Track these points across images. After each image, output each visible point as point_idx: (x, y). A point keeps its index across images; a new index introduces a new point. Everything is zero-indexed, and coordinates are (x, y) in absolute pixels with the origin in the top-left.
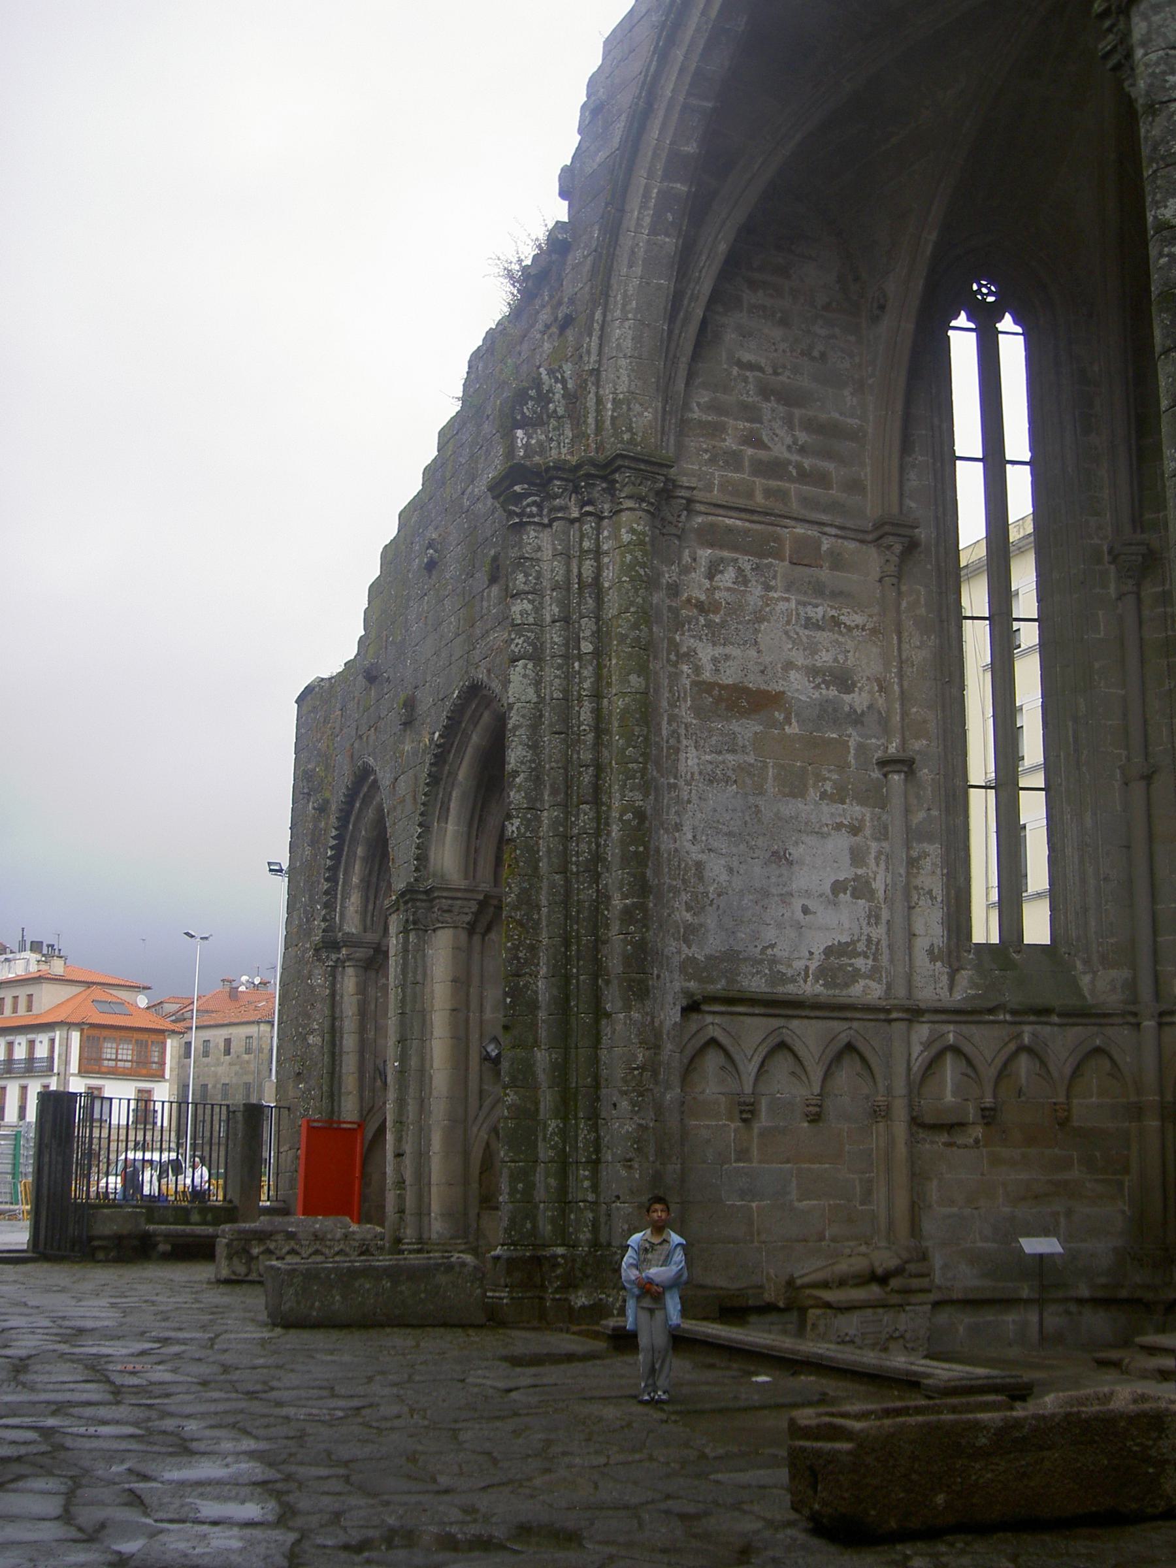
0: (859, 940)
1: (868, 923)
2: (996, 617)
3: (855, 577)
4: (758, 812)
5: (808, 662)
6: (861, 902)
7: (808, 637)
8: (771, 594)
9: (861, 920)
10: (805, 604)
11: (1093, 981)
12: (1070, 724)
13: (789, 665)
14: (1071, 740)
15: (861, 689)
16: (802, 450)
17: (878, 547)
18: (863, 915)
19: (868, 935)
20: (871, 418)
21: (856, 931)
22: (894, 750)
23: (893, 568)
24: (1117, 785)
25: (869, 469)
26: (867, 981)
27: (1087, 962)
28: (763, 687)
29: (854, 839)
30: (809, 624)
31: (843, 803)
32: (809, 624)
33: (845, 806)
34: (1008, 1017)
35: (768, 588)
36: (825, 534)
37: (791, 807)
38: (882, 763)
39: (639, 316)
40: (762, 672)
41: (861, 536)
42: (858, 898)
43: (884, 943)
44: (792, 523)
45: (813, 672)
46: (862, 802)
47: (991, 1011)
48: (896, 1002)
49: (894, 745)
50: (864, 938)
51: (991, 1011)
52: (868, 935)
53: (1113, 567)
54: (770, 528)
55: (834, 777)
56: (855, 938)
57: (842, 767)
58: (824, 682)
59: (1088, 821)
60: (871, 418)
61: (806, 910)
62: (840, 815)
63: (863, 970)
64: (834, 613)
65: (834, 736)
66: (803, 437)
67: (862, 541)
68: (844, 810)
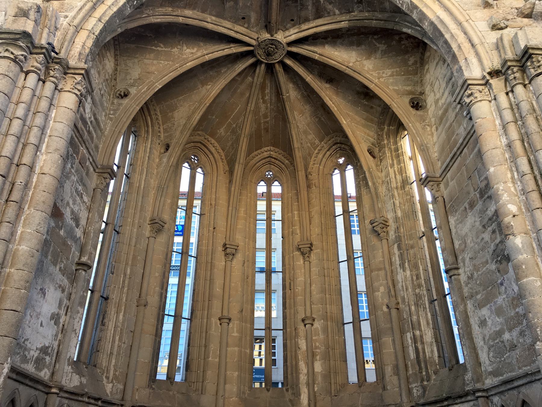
2: (111, 225)
3: (89, 182)
4: (43, 265)
6: (56, 327)
7: (75, 196)
8: (72, 170)
10: (78, 182)
11: (113, 387)
12: (122, 276)
13: (68, 203)
14: (121, 283)
15: (80, 228)
16: (91, 122)
17: (99, 176)
20: (108, 129)
21: (51, 342)
22: (85, 260)
23: (103, 187)
24: (134, 306)
25: (101, 146)
27: (108, 378)
28: (60, 207)
30: (76, 190)
32: (76, 190)
34: (86, 400)
35: (72, 167)
36: (89, 159)
37: (52, 268)
38: (78, 264)
39: (106, 25)
40: (62, 200)
41: (95, 168)
43: (56, 351)
44: (84, 147)
45: (73, 212)
46: (68, 278)
47: (82, 395)
48: (56, 383)
49: (86, 258)
50: (52, 346)
51: (82, 395)
53: (149, 226)
54: (79, 143)
57: (68, 259)
59: (121, 317)
60: (108, 129)
61: (41, 325)
64: (82, 191)
65: (69, 243)
66: (93, 119)
67: (94, 170)
68: (63, 279)
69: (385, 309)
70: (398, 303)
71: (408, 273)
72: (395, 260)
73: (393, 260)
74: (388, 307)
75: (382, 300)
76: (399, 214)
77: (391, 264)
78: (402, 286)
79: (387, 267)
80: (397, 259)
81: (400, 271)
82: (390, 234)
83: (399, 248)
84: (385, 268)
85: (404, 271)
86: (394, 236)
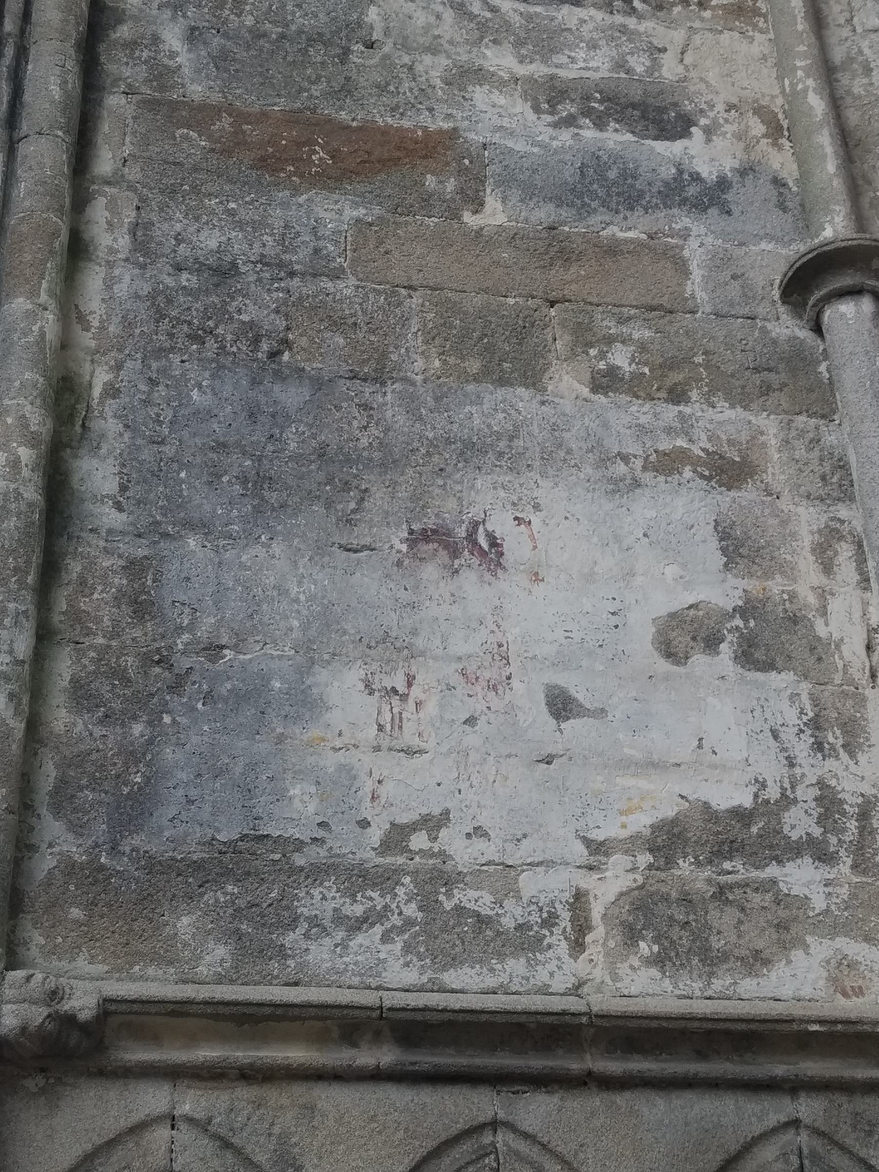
0: (786, 801)
1: (818, 746)
5: (537, 69)
9: (788, 735)
18: (791, 716)
19: (821, 784)
26: (841, 942)
29: (725, 499)
31: (677, 396)
33: (688, 410)
42: (768, 666)
50: (806, 794)
52: (821, 784)
55: (641, 333)
56: (773, 793)
58: (587, 112)
62: (669, 431)
63: (819, 903)
68: (681, 416)
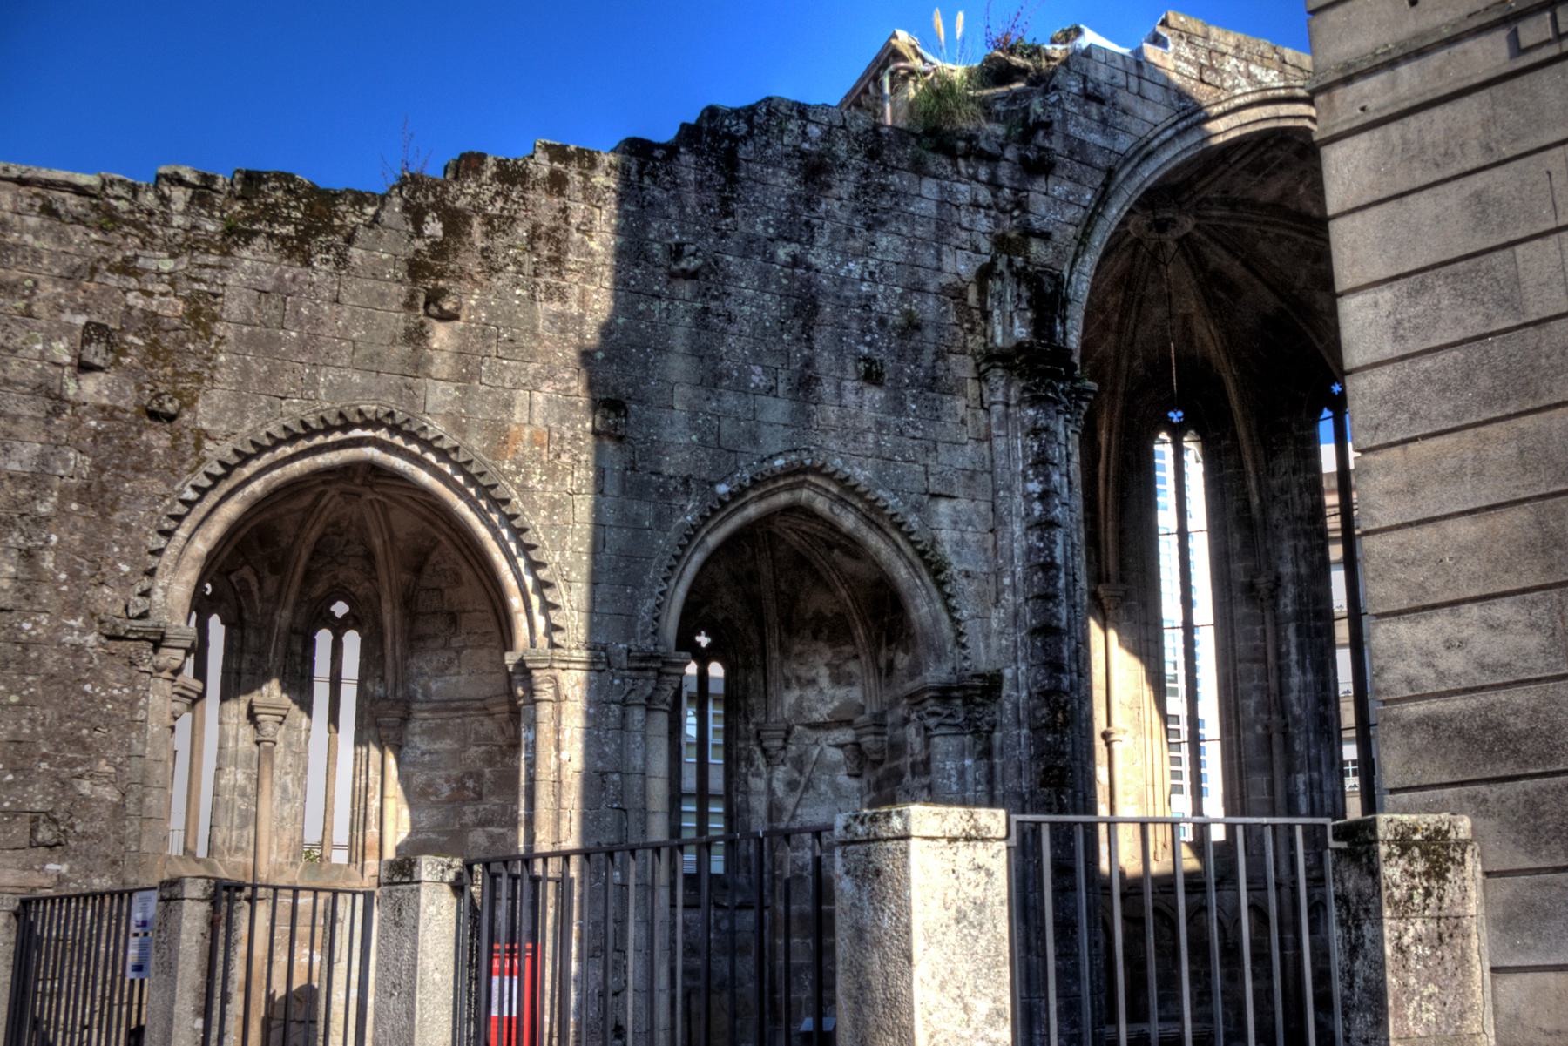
69: (1259, 729)
70: (1286, 725)
71: (1310, 677)
72: (1288, 653)
73: (1284, 649)
74: (1266, 727)
75: (1257, 713)
76: (1303, 570)
77: (1279, 655)
78: (1299, 699)
79: (1271, 658)
80: (1293, 650)
81: (1295, 670)
82: (1282, 603)
83: (1299, 631)
84: (1265, 661)
85: (1304, 673)
86: (1289, 609)
